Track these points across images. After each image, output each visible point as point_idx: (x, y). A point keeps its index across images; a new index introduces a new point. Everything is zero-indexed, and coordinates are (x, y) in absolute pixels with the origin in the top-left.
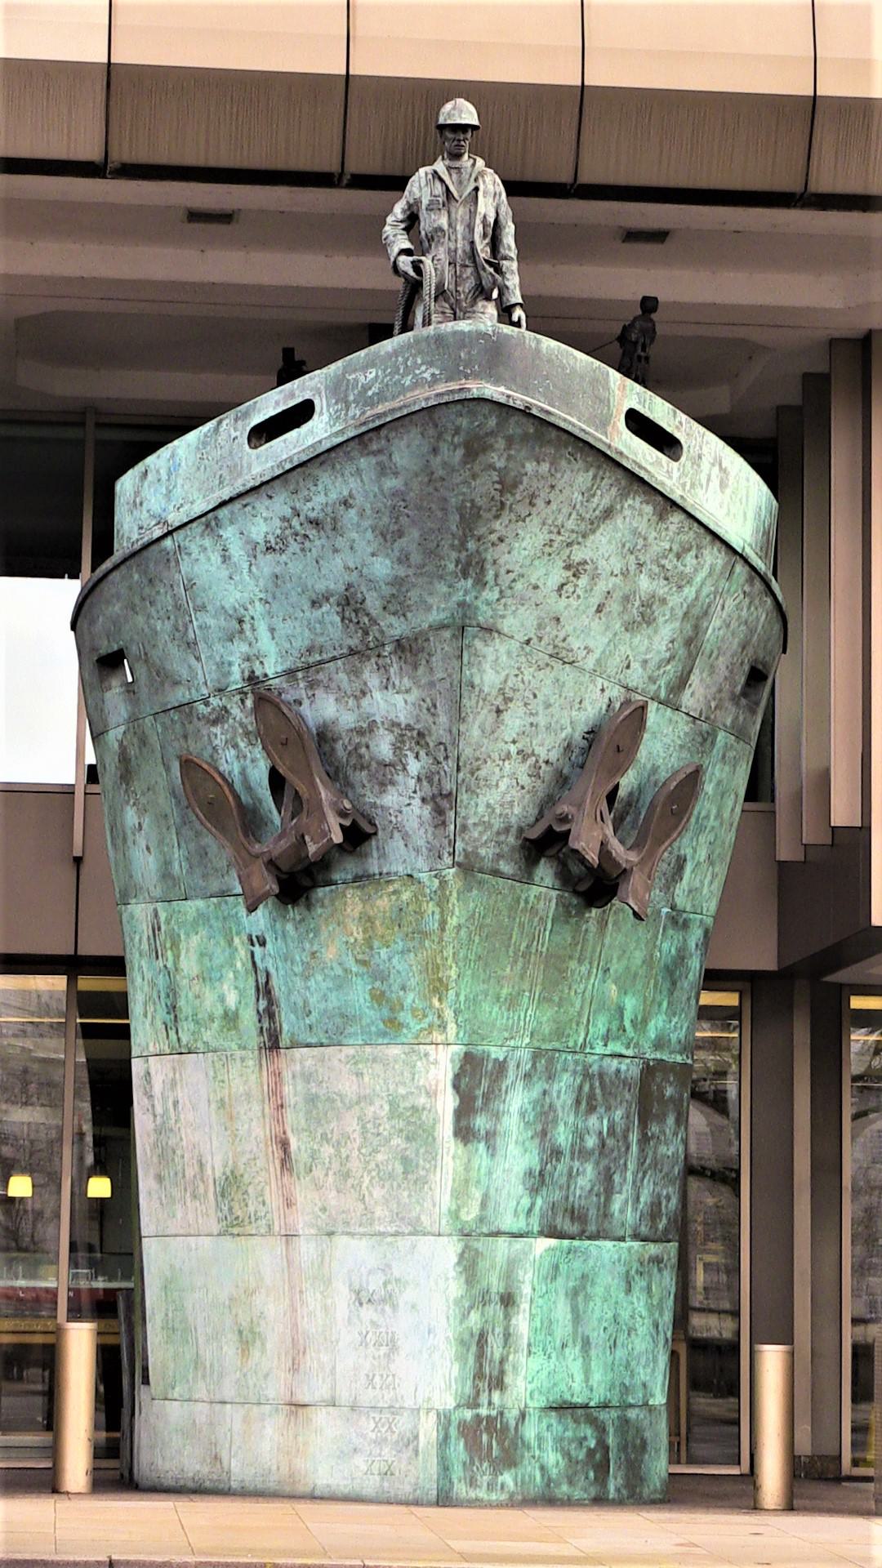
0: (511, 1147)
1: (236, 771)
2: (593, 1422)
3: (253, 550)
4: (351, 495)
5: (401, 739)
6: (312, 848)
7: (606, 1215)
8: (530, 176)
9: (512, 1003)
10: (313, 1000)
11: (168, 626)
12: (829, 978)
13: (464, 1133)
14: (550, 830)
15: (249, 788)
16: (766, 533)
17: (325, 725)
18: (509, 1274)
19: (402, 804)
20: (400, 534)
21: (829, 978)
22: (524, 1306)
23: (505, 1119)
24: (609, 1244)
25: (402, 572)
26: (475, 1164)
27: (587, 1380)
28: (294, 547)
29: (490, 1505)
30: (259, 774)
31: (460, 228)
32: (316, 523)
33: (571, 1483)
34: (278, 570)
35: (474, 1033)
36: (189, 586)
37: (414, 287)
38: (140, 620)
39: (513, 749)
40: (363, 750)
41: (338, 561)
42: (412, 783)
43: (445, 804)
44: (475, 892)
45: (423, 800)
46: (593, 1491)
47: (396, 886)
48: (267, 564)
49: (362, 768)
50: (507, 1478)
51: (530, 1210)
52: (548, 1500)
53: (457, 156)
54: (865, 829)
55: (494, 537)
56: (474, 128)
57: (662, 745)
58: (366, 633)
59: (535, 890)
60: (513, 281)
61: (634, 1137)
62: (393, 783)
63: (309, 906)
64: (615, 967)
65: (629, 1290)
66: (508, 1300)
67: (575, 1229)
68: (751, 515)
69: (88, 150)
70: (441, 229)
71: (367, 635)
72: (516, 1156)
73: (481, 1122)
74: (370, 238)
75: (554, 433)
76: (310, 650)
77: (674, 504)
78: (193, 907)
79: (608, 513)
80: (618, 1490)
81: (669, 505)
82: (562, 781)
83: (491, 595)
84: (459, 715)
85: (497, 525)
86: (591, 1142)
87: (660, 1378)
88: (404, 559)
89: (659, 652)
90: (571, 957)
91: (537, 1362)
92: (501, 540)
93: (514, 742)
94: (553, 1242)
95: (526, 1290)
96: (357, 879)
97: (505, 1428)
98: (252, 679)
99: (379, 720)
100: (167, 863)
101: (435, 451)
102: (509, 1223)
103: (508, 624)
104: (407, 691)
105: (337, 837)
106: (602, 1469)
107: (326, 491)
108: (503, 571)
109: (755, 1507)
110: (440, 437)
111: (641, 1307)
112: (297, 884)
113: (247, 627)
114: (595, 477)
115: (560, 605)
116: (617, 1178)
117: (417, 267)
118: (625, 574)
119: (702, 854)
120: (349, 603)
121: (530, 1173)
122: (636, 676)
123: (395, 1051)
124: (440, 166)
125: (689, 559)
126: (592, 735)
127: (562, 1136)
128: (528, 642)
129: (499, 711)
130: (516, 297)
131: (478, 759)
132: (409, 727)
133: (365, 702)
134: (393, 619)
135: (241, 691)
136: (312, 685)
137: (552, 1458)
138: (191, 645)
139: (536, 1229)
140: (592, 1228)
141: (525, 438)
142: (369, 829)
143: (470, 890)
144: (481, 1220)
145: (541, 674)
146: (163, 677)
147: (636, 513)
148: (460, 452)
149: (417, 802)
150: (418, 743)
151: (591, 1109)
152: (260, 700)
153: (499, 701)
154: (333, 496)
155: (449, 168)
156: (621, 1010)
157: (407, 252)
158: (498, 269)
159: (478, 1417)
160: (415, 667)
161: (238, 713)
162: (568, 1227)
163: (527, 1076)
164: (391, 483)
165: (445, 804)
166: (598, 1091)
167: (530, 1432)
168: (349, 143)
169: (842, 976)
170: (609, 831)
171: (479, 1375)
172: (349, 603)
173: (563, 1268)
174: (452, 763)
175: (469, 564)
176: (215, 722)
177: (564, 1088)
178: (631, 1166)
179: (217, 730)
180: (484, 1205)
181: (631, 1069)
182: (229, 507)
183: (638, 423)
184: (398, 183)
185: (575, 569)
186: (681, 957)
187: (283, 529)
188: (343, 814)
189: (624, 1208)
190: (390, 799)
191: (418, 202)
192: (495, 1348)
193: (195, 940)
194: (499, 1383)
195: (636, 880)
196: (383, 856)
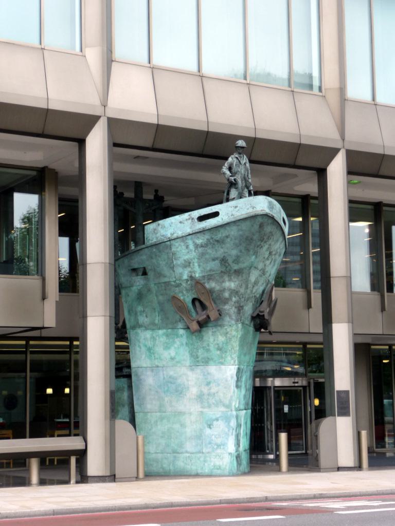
3: (196, 246)
4: (229, 235)
5: (231, 293)
10: (199, 354)
11: (164, 263)
14: (258, 315)
17: (211, 289)
19: (230, 308)
20: (240, 244)
25: (239, 254)
32: (218, 241)
34: (204, 252)
35: (240, 363)
36: (174, 254)
38: (154, 261)
40: (221, 295)
41: (222, 250)
42: (233, 303)
43: (241, 308)
45: (236, 307)
47: (226, 327)
48: (200, 250)
49: (220, 299)
58: (227, 268)
62: (228, 303)
69: (148, 144)
70: (239, 171)
71: (227, 268)
76: (210, 270)
78: (161, 332)
84: (247, 288)
85: (262, 244)
88: (241, 251)
99: (226, 288)
101: (253, 226)
104: (235, 282)
113: (191, 264)
120: (224, 261)
123: (223, 367)
132: (234, 290)
133: (224, 284)
134: (234, 265)
135: (187, 280)
136: (209, 279)
146: (159, 275)
149: (234, 308)
150: (236, 294)
154: (224, 235)
160: (239, 276)
164: (241, 233)
165: (241, 308)
172: (224, 261)
174: (244, 299)
176: (176, 287)
179: (177, 289)
182: (191, 236)
184: (226, 159)
187: (207, 242)
190: (227, 307)
193: (162, 339)
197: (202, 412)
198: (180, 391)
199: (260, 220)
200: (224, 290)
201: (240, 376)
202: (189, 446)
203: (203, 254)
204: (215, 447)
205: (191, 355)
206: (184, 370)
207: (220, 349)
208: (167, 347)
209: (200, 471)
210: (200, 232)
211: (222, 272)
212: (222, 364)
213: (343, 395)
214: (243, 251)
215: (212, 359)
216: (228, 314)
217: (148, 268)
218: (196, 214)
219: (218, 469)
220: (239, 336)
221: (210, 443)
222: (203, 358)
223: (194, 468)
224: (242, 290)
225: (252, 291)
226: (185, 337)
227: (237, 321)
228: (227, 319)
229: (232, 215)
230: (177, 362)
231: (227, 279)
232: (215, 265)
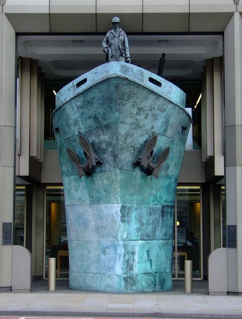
0: (133, 223)
1: (78, 150)
2: (152, 276)
5: (107, 144)
6: (90, 166)
7: (154, 235)
8: (129, 31)
9: (132, 195)
12: (217, 183)
13: (123, 221)
15: (80, 154)
16: (183, 100)
18: (133, 247)
19: (107, 157)
21: (217, 183)
22: (137, 254)
23: (131, 218)
24: (156, 241)
25: (105, 111)
26: (125, 226)
27: (151, 268)
28: (85, 107)
29: (130, 293)
30: (82, 151)
31: (116, 43)
32: (88, 102)
33: (148, 287)
35: (124, 202)
37: (107, 55)
43: (116, 157)
46: (153, 290)
48: (80, 110)
50: (134, 288)
51: (137, 236)
52: (143, 292)
53: (116, 28)
54: (214, 156)
56: (119, 23)
57: (162, 143)
59: (136, 173)
60: (128, 53)
61: (160, 220)
63: (92, 177)
64: (154, 187)
65: (160, 250)
66: (133, 253)
67: (148, 238)
68: (179, 97)
69: (47, 31)
72: (134, 225)
73: (126, 219)
74: (99, 44)
75: (132, 83)
76: (90, 127)
77: (160, 96)
78: (73, 177)
79: (146, 98)
80: (158, 289)
81: (159, 96)
82: (140, 151)
83: (123, 115)
84: (117, 139)
86: (151, 222)
87: (168, 267)
90: (144, 186)
91: (139, 265)
94: (143, 241)
95: (137, 251)
96: (101, 172)
97: (133, 278)
98: (79, 133)
100: (68, 168)
101: (109, 87)
102: (133, 238)
103: (126, 121)
105: (95, 164)
106: (155, 285)
107: (90, 96)
109: (184, 292)
110: (110, 85)
111: (163, 253)
112: (89, 172)
115: (138, 117)
116: (157, 228)
117: (108, 51)
118: (151, 110)
119: (173, 164)
121: (137, 228)
122: (155, 130)
123: (109, 205)
124: (112, 31)
125: (165, 106)
126: (146, 142)
127: (145, 221)
128: (131, 124)
129: (126, 138)
130: (128, 56)
132: (108, 142)
133: (100, 137)
134: (104, 121)
135: (78, 135)
136: (90, 134)
137: (144, 283)
138: (69, 126)
139: (139, 239)
140: (152, 238)
141: (127, 84)
142: (102, 162)
144: (127, 237)
146: (65, 133)
147: (152, 97)
148: (114, 87)
149: (111, 157)
151: (150, 215)
152: (80, 137)
153: (125, 136)
154: (91, 97)
155: (114, 31)
156: (156, 195)
157: (107, 48)
158: (125, 51)
159: (127, 276)
161: (78, 140)
162: (145, 238)
163: (136, 209)
164: (102, 94)
166: (152, 212)
167: (139, 278)
168: (95, 28)
169: (219, 183)
170: (150, 161)
171: (128, 268)
172: (96, 118)
173: (145, 246)
175: (117, 110)
177: (144, 211)
178: (160, 225)
179: (74, 143)
180: (127, 235)
181: (159, 207)
183: (151, 80)
184: (105, 34)
185: (140, 110)
186: (170, 184)
188: (96, 159)
189: (159, 234)
190: (106, 156)
191: (108, 38)
192: (131, 262)
194: (132, 269)
195: (156, 170)
196: (105, 167)
197: (99, 241)
198: (85, 224)
199: (114, 82)
200: (101, 142)
201: (126, 212)
202: (93, 269)
203: (82, 114)
204: (108, 269)
205: (90, 196)
206: (87, 208)
207: (105, 191)
208: (76, 190)
209: (98, 288)
210: (77, 96)
211: (97, 127)
212: (108, 203)
213: (232, 229)
214: (107, 109)
215: (102, 199)
216: (107, 161)
217: (60, 128)
218: (76, 81)
219: (109, 287)
220: (118, 180)
221: (105, 266)
222: (97, 198)
223: (95, 285)
224: (114, 142)
225: (125, 142)
226: (84, 181)
227: (115, 167)
228: (107, 166)
229: (94, 80)
230: (83, 201)
231: (101, 133)
232: (91, 122)
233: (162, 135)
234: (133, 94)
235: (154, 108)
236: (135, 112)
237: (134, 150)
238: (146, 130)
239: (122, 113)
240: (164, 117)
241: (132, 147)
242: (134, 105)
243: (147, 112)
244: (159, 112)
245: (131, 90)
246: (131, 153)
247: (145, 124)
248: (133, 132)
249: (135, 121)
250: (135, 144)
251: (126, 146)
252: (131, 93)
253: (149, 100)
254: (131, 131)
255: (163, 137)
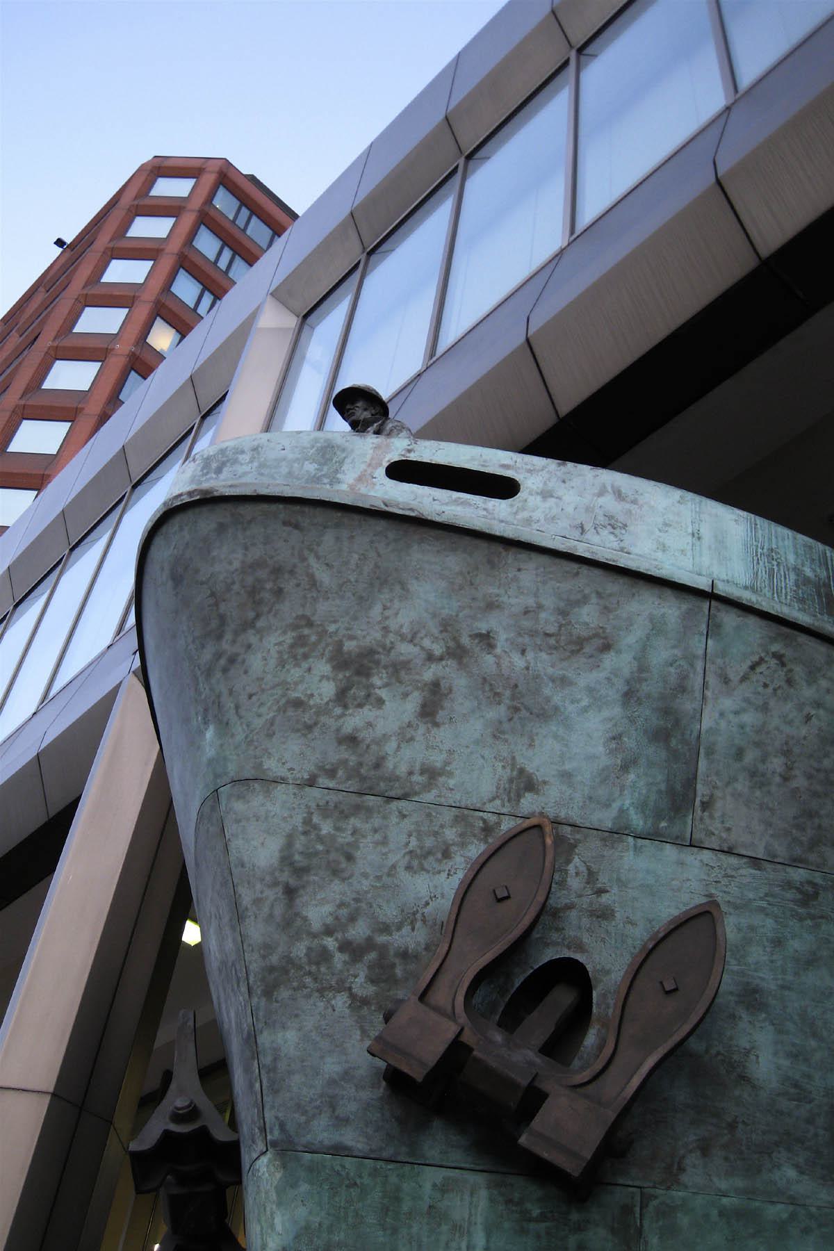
39: (330, 943)
44: (304, 1187)
55: (223, 662)
85: (225, 645)
89: (591, 758)
92: (232, 660)
93: (329, 931)
103: (272, 766)
108: (243, 698)
114: (338, 539)
115: (354, 721)
128: (311, 782)
129: (290, 892)
131: (272, 969)
141: (222, 528)
143: (294, 1186)
145: (354, 822)
153: (285, 877)
225: (291, 923)
233: (653, 836)
234: (277, 571)
235: (486, 640)
236: (328, 690)
237: (382, 973)
238: (463, 814)
239: (233, 718)
240: (613, 694)
241: (354, 951)
242: (301, 641)
243: (428, 675)
244: (543, 662)
245: (256, 553)
246: (359, 1004)
247: (437, 759)
248: (345, 838)
249: (344, 753)
250: (385, 929)
251: (300, 950)
252: (262, 574)
253: (414, 586)
254: (326, 828)
255: (670, 852)
